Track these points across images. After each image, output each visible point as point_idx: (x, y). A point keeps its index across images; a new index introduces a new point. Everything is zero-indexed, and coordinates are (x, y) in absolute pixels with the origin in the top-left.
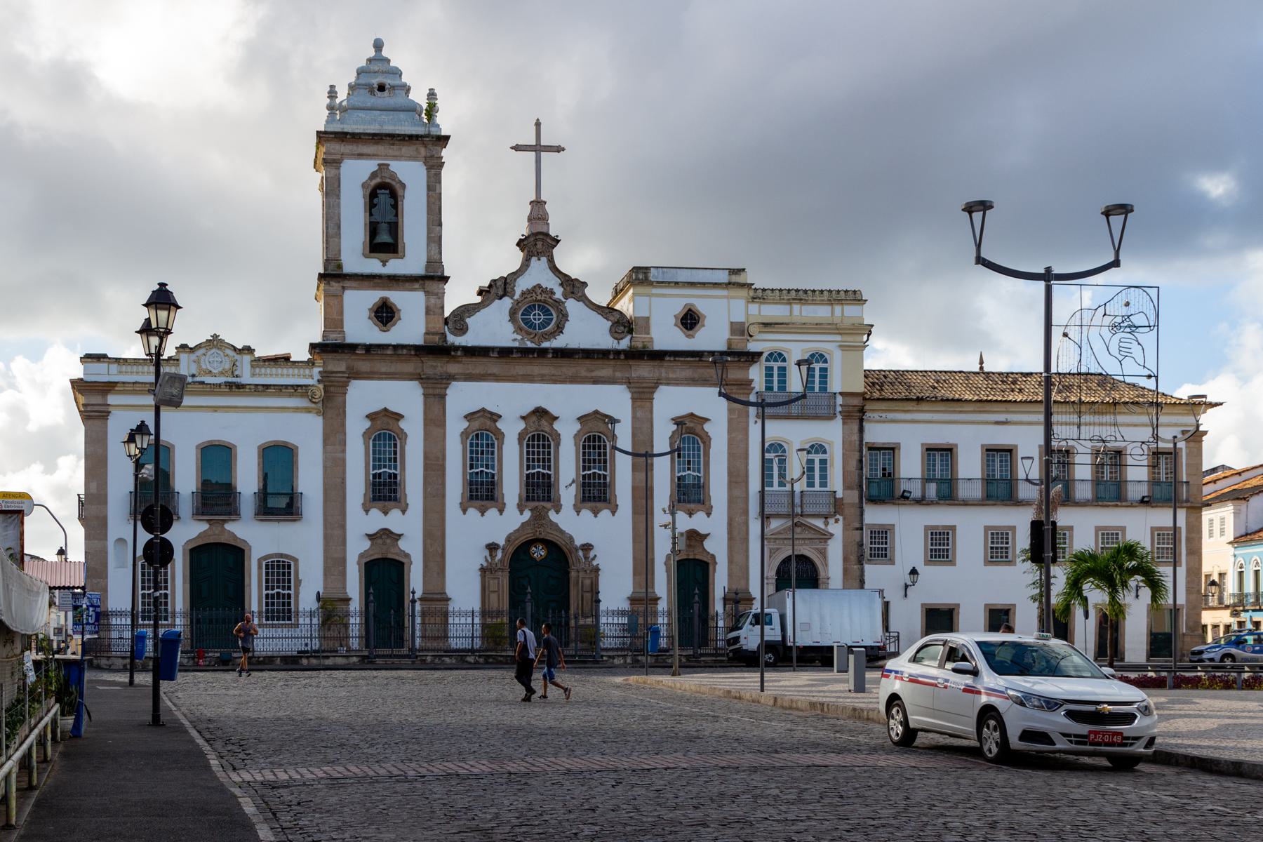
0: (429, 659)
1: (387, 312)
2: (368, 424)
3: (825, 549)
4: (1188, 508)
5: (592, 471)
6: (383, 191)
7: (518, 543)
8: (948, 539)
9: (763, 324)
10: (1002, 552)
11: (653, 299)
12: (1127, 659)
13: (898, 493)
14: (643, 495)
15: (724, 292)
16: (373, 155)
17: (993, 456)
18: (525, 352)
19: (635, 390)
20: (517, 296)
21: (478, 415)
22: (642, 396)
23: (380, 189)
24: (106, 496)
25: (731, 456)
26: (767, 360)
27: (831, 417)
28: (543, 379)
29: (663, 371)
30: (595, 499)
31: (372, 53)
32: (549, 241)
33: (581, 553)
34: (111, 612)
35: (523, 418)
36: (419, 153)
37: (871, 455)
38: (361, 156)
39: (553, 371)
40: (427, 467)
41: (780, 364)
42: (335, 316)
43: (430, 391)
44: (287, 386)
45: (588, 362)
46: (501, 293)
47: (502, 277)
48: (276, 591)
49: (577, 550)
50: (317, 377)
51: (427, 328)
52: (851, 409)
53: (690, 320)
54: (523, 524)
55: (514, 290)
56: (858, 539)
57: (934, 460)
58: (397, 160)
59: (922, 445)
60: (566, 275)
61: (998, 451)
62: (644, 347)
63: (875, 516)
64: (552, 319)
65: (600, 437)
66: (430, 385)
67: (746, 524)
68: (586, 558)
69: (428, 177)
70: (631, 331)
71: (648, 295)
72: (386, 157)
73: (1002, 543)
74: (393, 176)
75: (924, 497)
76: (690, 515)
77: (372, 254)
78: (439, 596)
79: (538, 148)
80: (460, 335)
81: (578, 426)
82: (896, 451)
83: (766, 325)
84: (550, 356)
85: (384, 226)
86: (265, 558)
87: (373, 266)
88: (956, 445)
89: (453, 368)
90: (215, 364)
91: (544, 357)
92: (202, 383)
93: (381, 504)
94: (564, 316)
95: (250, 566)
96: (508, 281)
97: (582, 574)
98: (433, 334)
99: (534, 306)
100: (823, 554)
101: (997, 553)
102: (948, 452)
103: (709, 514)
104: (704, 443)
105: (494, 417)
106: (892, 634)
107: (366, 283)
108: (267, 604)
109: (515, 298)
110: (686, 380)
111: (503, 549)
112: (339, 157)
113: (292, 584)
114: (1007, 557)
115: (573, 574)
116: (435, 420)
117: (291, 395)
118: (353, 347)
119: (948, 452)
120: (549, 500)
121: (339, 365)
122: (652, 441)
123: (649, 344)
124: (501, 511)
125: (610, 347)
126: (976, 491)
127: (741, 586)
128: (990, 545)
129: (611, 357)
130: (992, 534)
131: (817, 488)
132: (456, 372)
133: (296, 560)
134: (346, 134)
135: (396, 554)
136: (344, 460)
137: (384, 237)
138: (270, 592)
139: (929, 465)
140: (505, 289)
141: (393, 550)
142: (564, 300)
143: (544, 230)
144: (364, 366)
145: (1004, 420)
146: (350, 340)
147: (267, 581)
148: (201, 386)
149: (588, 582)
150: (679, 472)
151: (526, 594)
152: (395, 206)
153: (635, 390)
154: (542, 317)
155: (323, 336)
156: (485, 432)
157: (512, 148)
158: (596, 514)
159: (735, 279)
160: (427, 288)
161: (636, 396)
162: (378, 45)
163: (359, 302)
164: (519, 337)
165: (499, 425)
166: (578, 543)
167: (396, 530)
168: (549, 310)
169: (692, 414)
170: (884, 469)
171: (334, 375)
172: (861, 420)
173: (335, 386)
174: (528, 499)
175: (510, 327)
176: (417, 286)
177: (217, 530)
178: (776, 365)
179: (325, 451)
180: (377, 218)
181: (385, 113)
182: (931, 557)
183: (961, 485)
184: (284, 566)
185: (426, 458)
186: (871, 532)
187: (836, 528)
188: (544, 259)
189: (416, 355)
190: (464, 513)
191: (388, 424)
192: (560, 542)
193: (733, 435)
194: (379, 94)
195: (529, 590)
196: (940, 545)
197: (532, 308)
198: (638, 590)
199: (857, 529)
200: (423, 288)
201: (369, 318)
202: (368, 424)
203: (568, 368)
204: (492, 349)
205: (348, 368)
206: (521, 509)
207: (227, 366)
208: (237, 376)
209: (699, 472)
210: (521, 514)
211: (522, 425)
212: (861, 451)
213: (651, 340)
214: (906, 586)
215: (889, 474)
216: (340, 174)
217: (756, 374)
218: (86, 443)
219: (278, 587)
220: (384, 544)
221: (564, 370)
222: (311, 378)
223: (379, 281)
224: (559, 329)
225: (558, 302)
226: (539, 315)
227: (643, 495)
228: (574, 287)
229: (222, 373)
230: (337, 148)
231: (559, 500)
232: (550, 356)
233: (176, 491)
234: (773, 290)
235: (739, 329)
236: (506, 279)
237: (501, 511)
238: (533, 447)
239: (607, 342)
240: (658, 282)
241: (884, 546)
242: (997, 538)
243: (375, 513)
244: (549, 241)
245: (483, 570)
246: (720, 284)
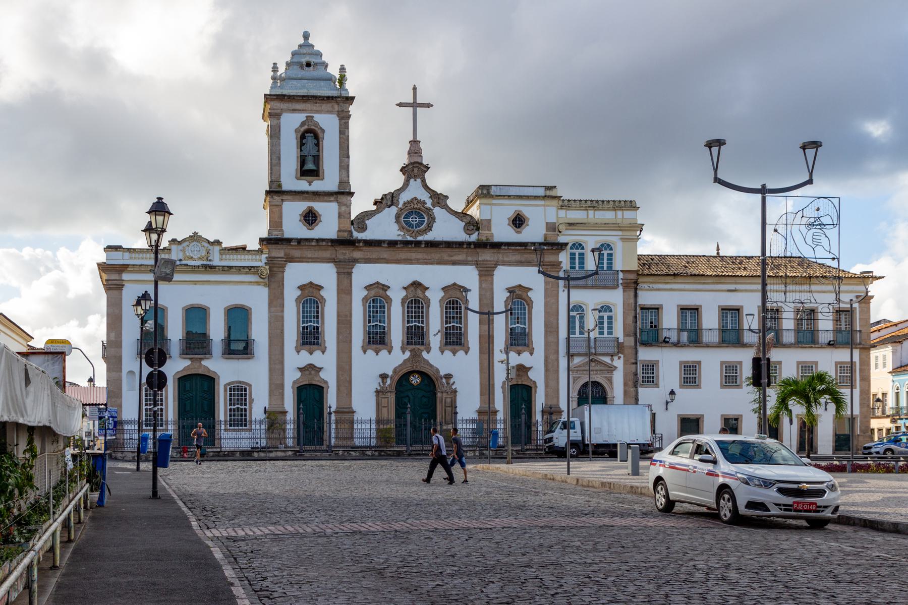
0: (341, 453)
1: (312, 217)
2: (299, 293)
3: (611, 377)
4: (860, 348)
5: (452, 324)
6: (309, 134)
7: (401, 373)
8: (696, 370)
9: (569, 224)
10: (733, 379)
11: (493, 207)
12: (819, 452)
13: (661, 339)
14: (487, 341)
15: (542, 202)
16: (303, 110)
17: (727, 313)
18: (406, 243)
19: (481, 269)
20: (400, 206)
21: (374, 286)
22: (486, 273)
23: (308, 133)
24: (121, 342)
25: (547, 314)
26: (571, 248)
27: (615, 287)
28: (418, 262)
29: (500, 256)
30: (454, 344)
31: (302, 41)
33: (444, 380)
34: (125, 421)
35: (405, 288)
36: (334, 108)
37: (642, 313)
38: (294, 111)
39: (425, 256)
40: (339, 322)
41: (580, 251)
42: (277, 220)
44: (244, 267)
45: (449, 250)
46: (389, 203)
47: (391, 193)
48: (237, 406)
49: (441, 378)
50: (264, 261)
51: (339, 227)
52: (629, 281)
53: (518, 221)
55: (398, 201)
56: (634, 370)
57: (686, 316)
58: (319, 113)
59: (678, 306)
60: (434, 191)
61: (730, 310)
62: (487, 239)
63: (646, 354)
64: (424, 221)
65: (457, 301)
66: (341, 266)
67: (557, 360)
68: (448, 383)
69: (340, 125)
70: (478, 229)
71: (490, 205)
72: (311, 111)
73: (733, 373)
74: (316, 124)
75: (679, 341)
76: (519, 354)
77: (302, 178)
78: (347, 410)
79: (415, 105)
80: (362, 232)
81: (442, 294)
82: (660, 310)
83: (570, 224)
84: (423, 246)
85: (310, 159)
86: (229, 384)
87: (303, 185)
88: (701, 306)
89: (357, 254)
90: (196, 252)
91: (419, 247)
92: (187, 265)
93: (308, 347)
94: (432, 219)
95: (219, 389)
96: (394, 195)
97: (445, 395)
98: (344, 231)
99: (412, 212)
100: (610, 380)
101: (729, 379)
102: (696, 310)
103: (531, 354)
104: (528, 305)
105: (385, 288)
106: (657, 435)
107: (298, 197)
108: (230, 416)
110: (516, 262)
111: (391, 378)
112: (279, 111)
113: (248, 402)
114: (736, 382)
115: (439, 395)
116: (344, 290)
117: (247, 273)
118: (289, 240)
119: (696, 310)
120: (422, 344)
121: (279, 252)
122: (493, 304)
123: (490, 238)
124: (390, 352)
125: (464, 240)
126: (715, 338)
127: (553, 403)
128: (724, 374)
129: (465, 246)
130: (726, 367)
131: (606, 335)
132: (359, 257)
133: (250, 386)
134: (284, 96)
135: (318, 381)
136: (283, 317)
137: (310, 166)
138: (232, 407)
139: (682, 319)
140: (392, 200)
141: (316, 379)
142: (432, 208)
143: (419, 161)
144: (296, 253)
145: (734, 289)
146: (287, 235)
147: (230, 400)
148: (186, 267)
149: (449, 400)
150: (511, 325)
151: (407, 408)
152: (318, 145)
153: (481, 269)
154: (418, 220)
155: (269, 233)
156: (379, 298)
158: (454, 353)
159: (549, 193)
160: (340, 200)
161: (482, 273)
162: (306, 36)
163: (293, 210)
164: (402, 233)
165: (388, 293)
166: (442, 373)
168: (422, 215)
169: (520, 286)
170: (652, 323)
171: (276, 259)
172: (636, 289)
173: (277, 267)
174: (408, 343)
175: (396, 227)
176: (332, 199)
177: (196, 365)
178: (577, 252)
179: (270, 311)
180: (305, 153)
181: (311, 81)
182: (684, 383)
183: (704, 332)
184: (242, 389)
185: (338, 316)
186: (643, 365)
187: (619, 363)
188: (419, 180)
189: (332, 246)
190: (365, 353)
191: (313, 292)
192: (430, 373)
193: (548, 300)
194: (307, 68)
195: (409, 406)
196: (690, 374)
197: (410, 213)
198: (483, 405)
199: (633, 363)
200: (337, 201)
201: (300, 221)
202: (299, 293)
203: (435, 254)
204: (384, 241)
205: (285, 255)
206: (403, 350)
207: (204, 253)
208: (210, 261)
209: (525, 325)
210: (404, 353)
211: (404, 293)
212: (636, 310)
213: (492, 235)
214: (667, 403)
215: (655, 326)
216: (280, 123)
217: (564, 258)
218: (108, 306)
219: (238, 404)
220: (310, 374)
221: (433, 255)
222: (261, 261)
223: (307, 195)
224: (429, 228)
225: (428, 209)
226: (416, 218)
227: (487, 341)
228: (439, 199)
229: (200, 259)
230: (278, 105)
232: (423, 246)
233: (211, 338)
234: (575, 201)
235: (552, 227)
236: (393, 194)
237: (390, 352)
238: (412, 308)
239: (461, 236)
240: (497, 196)
241: (652, 375)
242: (729, 370)
243: (304, 353)
245: (377, 392)
246: (539, 197)
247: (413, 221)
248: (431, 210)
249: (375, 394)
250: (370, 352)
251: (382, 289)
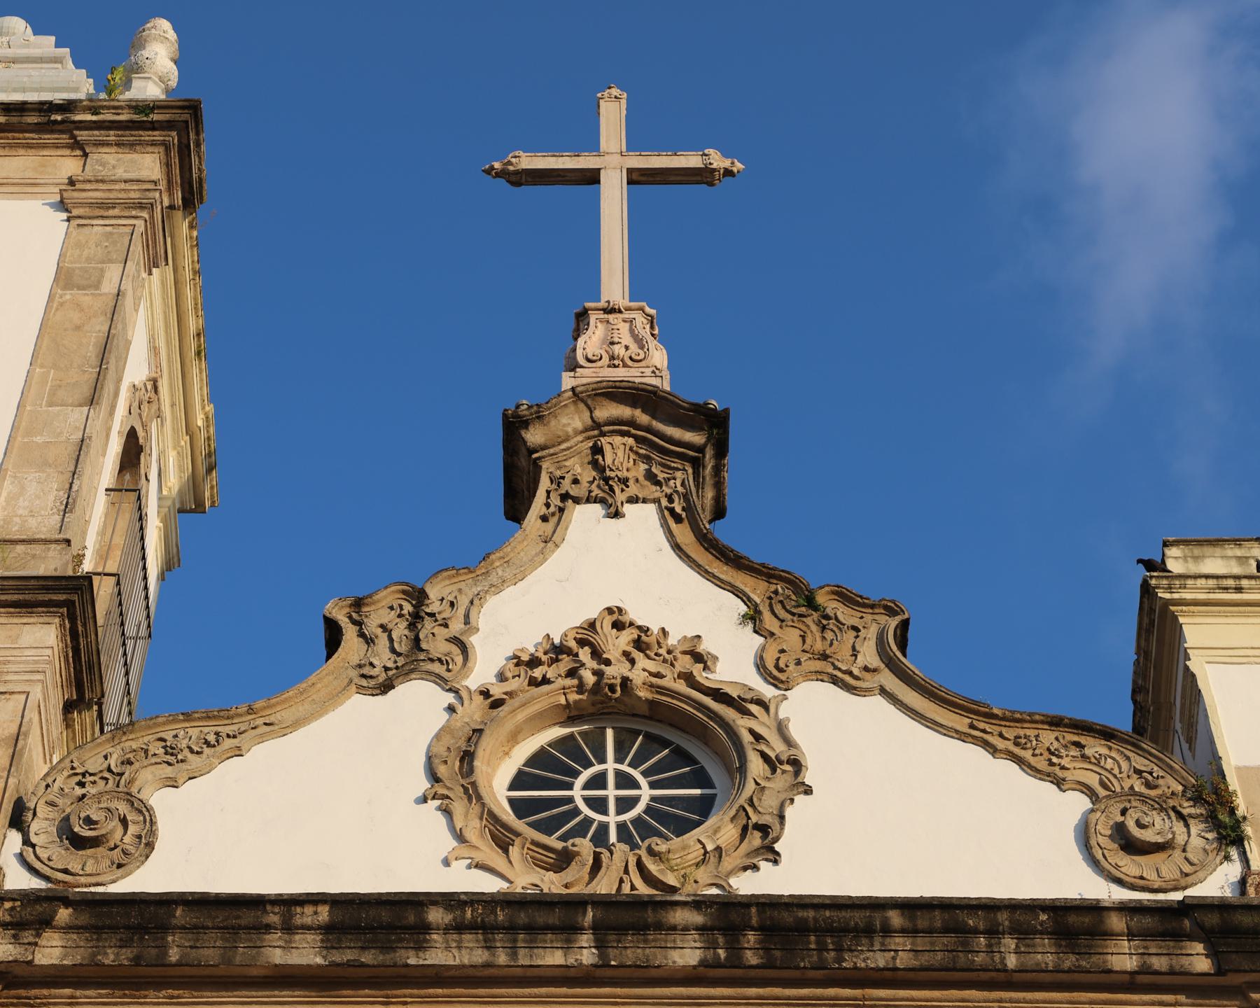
46: (382, 657)
142: (768, 692)
247: (599, 805)
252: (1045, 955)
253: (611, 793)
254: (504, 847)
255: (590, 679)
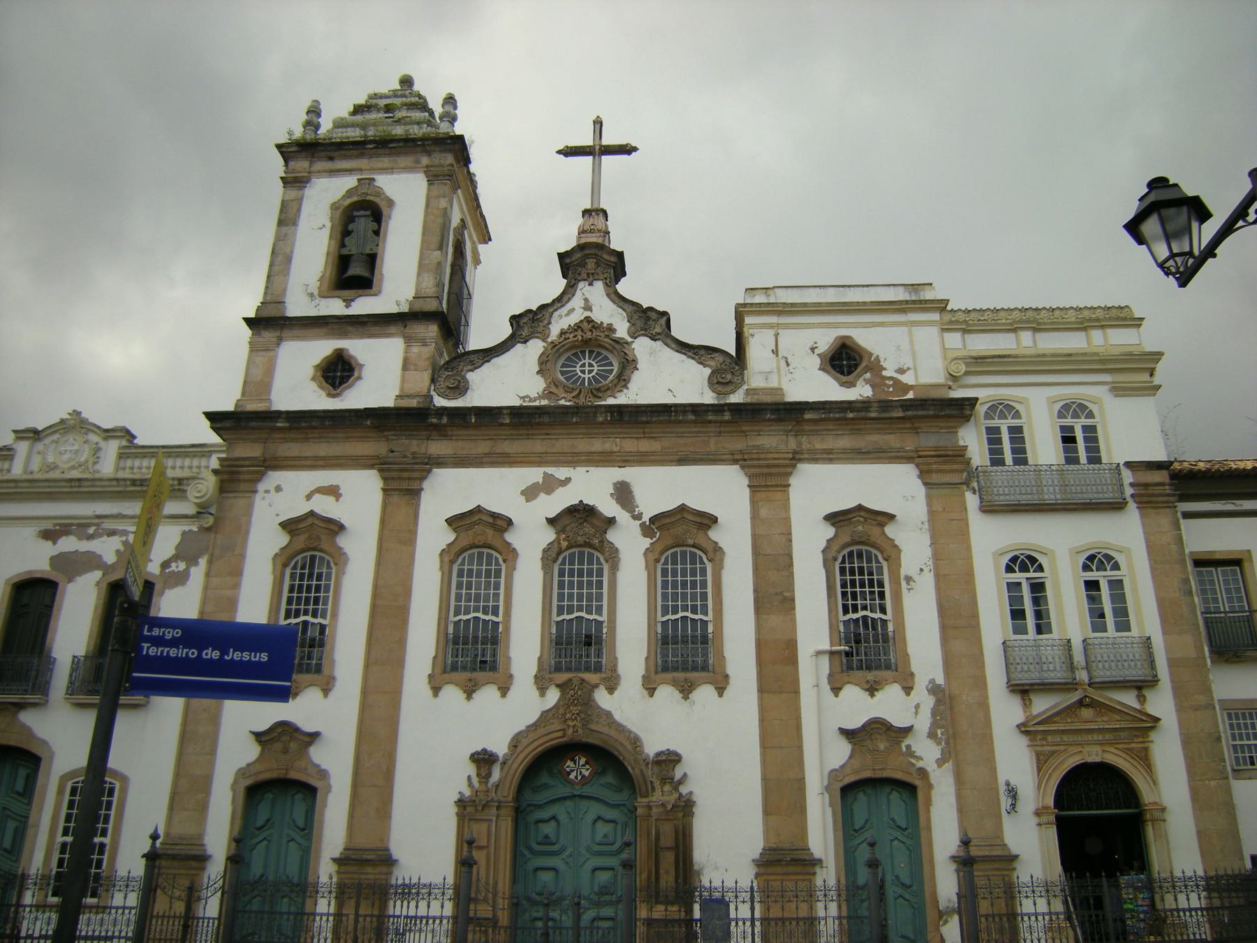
1: (343, 370)
6: (362, 213)
23: (358, 210)
26: (988, 416)
32: (606, 256)
37: (1200, 574)
38: (333, 173)
43: (395, 485)
51: (402, 389)
54: (544, 714)
64: (613, 370)
67: (984, 705)
74: (379, 192)
76: (872, 690)
82: (1246, 565)
87: (335, 307)
89: (437, 447)
94: (629, 364)
105: (499, 522)
109: (549, 340)
124: (504, 691)
137: (355, 270)
142: (630, 340)
153: (757, 471)
154: (596, 368)
157: (559, 152)
165: (510, 537)
167: (308, 727)
168: (606, 358)
176: (392, 329)
180: (352, 247)
217: (972, 440)
220: (286, 751)
224: (622, 381)
226: (590, 365)
230: (301, 165)
231: (614, 669)
237: (504, 691)
244: (606, 256)
247: (583, 372)
248: (627, 343)
249: (456, 810)
250: (452, 694)
251: (493, 526)
252: (691, 417)
253: (587, 368)
254: (557, 386)
255: (580, 338)
